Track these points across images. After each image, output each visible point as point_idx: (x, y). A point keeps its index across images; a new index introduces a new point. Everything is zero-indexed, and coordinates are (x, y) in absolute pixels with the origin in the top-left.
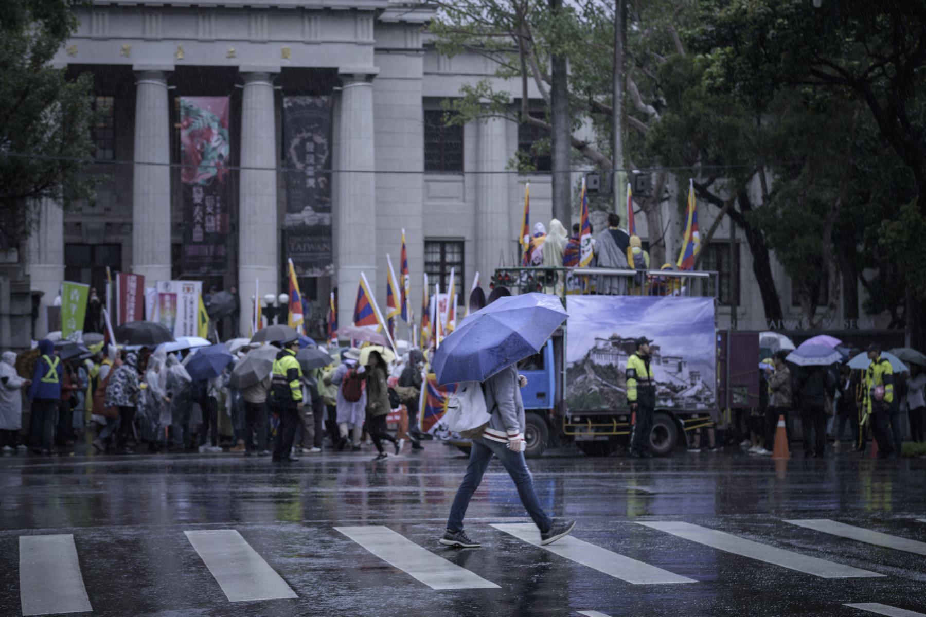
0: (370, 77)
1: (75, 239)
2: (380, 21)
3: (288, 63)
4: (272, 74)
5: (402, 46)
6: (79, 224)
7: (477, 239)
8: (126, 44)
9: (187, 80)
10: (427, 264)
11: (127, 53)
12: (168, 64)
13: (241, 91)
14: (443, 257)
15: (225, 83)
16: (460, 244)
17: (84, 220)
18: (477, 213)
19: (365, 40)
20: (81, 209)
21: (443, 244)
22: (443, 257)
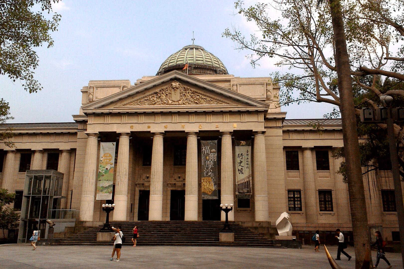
0: (263, 133)
1: (174, 189)
2: (267, 118)
3: (236, 129)
4: (230, 132)
5: (275, 126)
6: (175, 184)
7: (305, 190)
8: (183, 124)
9: (203, 136)
10: (289, 198)
11: (183, 127)
12: (197, 130)
13: (221, 139)
14: (294, 195)
15: (216, 136)
16: (299, 191)
17: (176, 183)
18: (304, 182)
19: (261, 121)
20: (175, 179)
22: (294, 195)
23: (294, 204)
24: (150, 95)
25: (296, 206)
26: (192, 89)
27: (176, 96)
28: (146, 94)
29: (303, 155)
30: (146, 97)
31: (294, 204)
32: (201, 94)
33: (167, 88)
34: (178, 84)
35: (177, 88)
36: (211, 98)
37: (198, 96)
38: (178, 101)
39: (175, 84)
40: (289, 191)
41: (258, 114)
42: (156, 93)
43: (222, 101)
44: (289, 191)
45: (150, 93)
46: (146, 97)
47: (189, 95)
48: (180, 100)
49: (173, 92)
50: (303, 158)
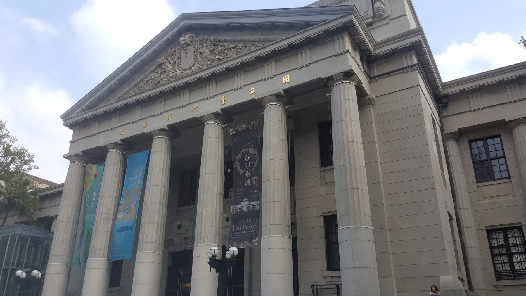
10: (492, 248)
14: (506, 240)
21: (505, 230)
22: (506, 240)
23: (511, 263)
25: (517, 267)
26: (211, 38)
27: (188, 59)
28: (147, 73)
29: (512, 138)
30: (146, 77)
32: (228, 41)
33: (175, 51)
34: (187, 36)
35: (188, 45)
36: (245, 41)
37: (221, 46)
38: (190, 69)
39: (185, 38)
40: (491, 231)
41: (334, 40)
42: (161, 65)
43: (263, 41)
44: (491, 231)
45: (152, 69)
46: (146, 77)
47: (206, 50)
48: (194, 66)
50: (514, 149)
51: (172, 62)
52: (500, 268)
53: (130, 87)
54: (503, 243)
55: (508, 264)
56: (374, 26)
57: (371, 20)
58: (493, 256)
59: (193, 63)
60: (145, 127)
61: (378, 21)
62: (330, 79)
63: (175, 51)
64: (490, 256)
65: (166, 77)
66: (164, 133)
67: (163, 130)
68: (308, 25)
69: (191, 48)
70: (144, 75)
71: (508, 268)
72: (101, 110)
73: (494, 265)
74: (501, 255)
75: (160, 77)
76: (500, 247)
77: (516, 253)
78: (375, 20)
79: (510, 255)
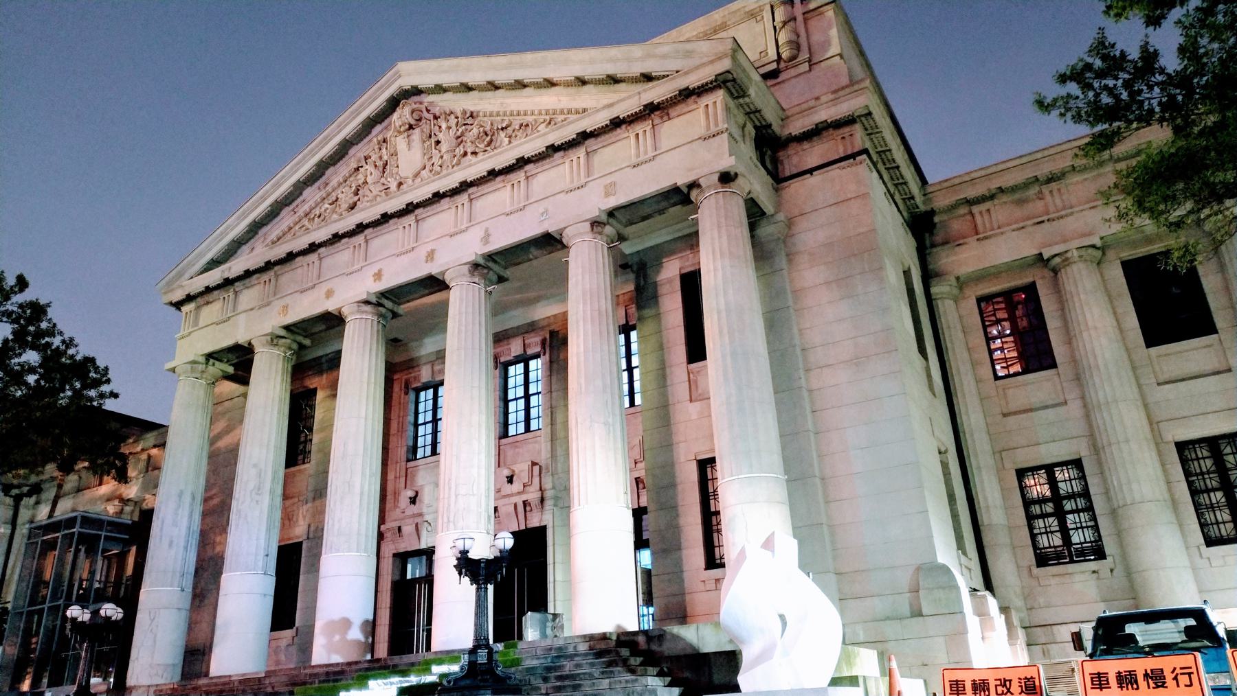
10: (1027, 503)
23: (1065, 531)
24: (340, 184)
31: (1065, 531)
35: (411, 127)
38: (417, 175)
49: (401, 143)
51: (380, 164)
52: (1043, 541)
53: (296, 218)
54: (1048, 494)
55: (1059, 534)
56: (783, 76)
57: (774, 66)
58: (1030, 518)
59: (419, 166)
60: (329, 294)
61: (787, 68)
62: (694, 185)
63: (385, 141)
64: (1023, 520)
65: (368, 193)
66: (368, 308)
67: (367, 302)
68: (647, 78)
69: (417, 131)
70: (323, 193)
71: (1057, 540)
72: (235, 267)
73: (1033, 537)
74: (1044, 516)
75: (356, 194)
76: (1041, 501)
77: (1072, 512)
78: (782, 65)
79: (1060, 514)
